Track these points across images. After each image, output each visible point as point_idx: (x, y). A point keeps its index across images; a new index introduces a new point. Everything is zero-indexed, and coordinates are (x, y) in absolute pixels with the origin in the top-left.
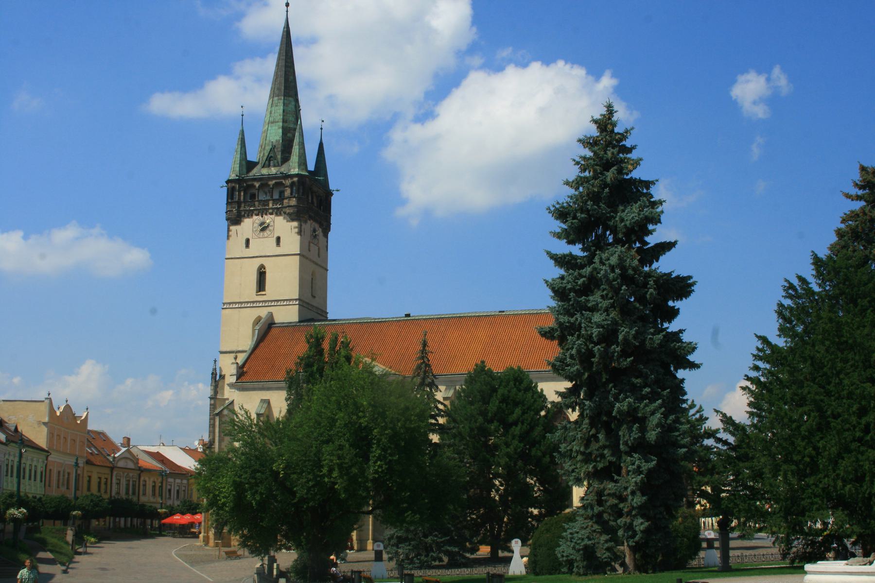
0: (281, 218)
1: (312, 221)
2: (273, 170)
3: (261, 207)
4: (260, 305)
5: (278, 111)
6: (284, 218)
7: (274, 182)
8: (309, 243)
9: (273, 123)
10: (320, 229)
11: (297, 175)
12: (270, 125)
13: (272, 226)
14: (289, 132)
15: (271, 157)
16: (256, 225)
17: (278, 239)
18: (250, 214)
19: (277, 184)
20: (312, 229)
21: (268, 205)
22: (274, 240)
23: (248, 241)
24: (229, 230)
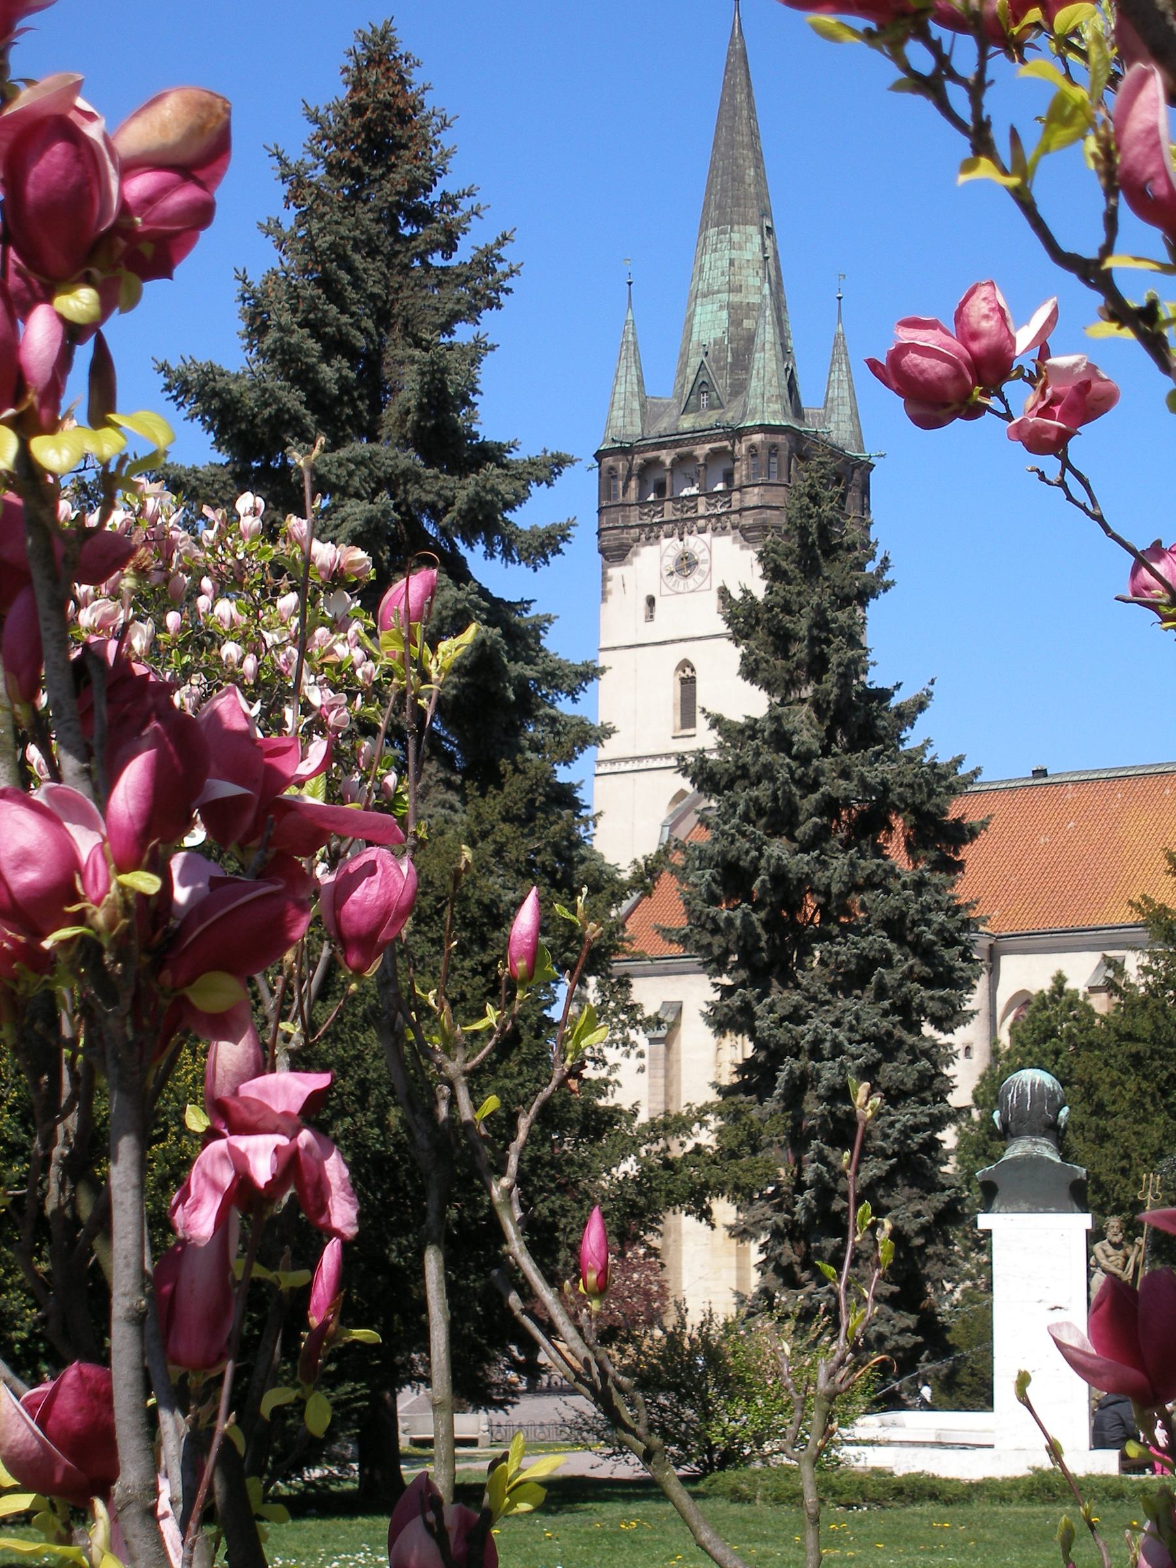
2: (709, 419)
3: (679, 515)
5: (719, 263)
6: (735, 540)
7: (708, 447)
9: (705, 296)
12: (699, 301)
13: (704, 562)
14: (748, 318)
18: (651, 533)
19: (715, 454)
21: (695, 507)
23: (651, 601)
24: (605, 579)
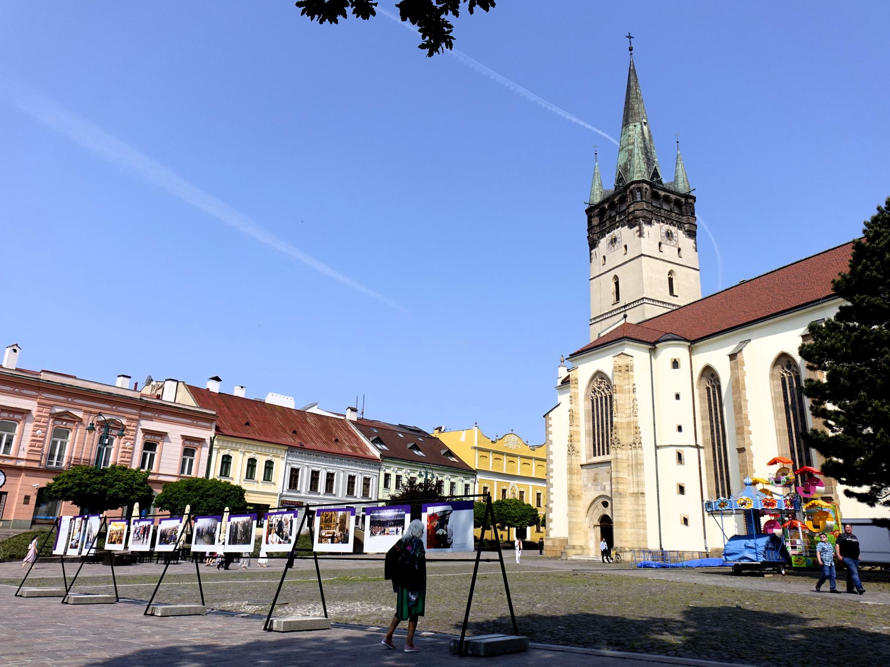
0: (626, 227)
1: (661, 224)
4: (615, 313)
8: (660, 244)
10: (680, 232)
11: (633, 183)
13: (619, 238)
15: (621, 179)
16: (608, 242)
17: (626, 247)
20: (664, 231)
22: (624, 248)
23: (604, 257)
24: (591, 254)
